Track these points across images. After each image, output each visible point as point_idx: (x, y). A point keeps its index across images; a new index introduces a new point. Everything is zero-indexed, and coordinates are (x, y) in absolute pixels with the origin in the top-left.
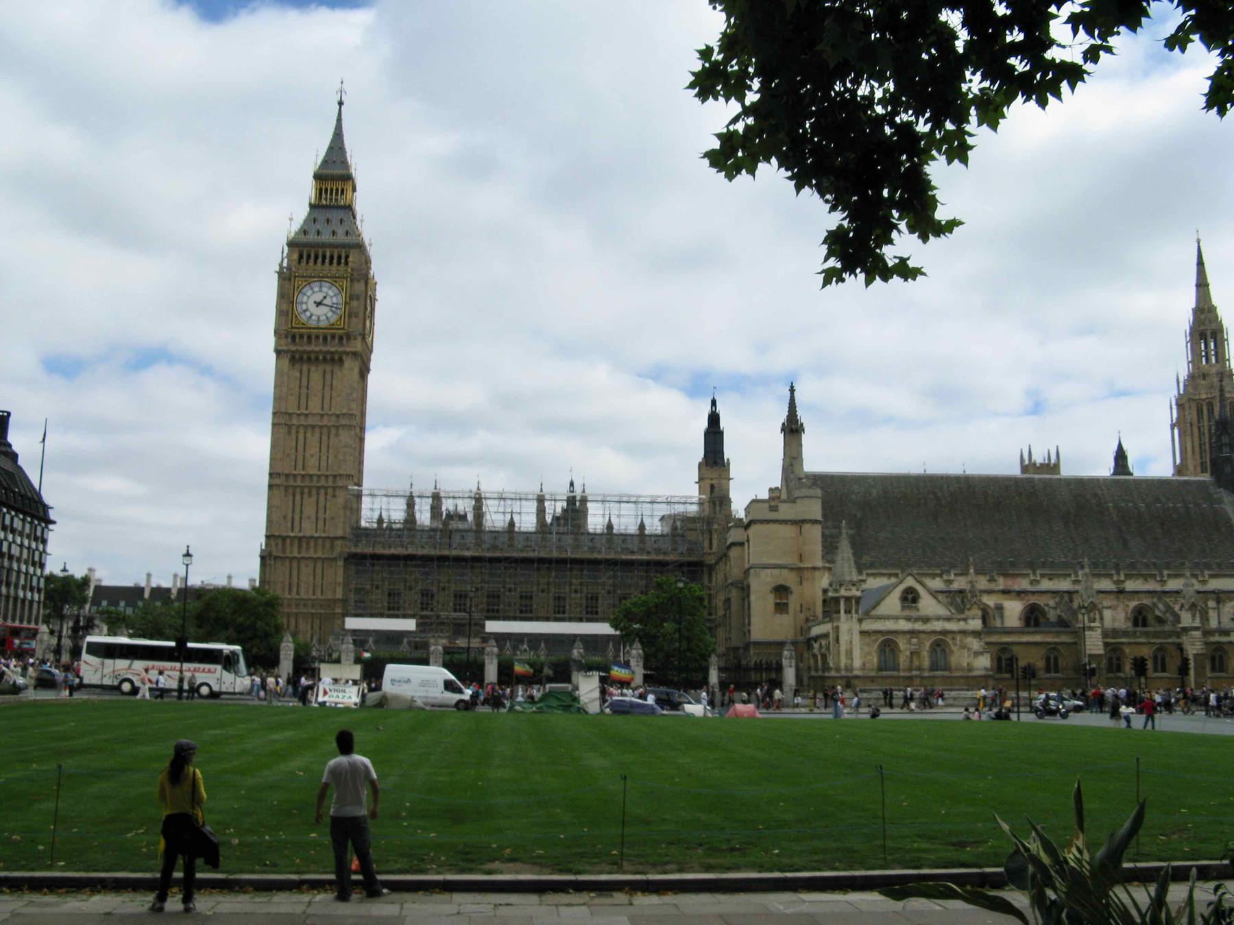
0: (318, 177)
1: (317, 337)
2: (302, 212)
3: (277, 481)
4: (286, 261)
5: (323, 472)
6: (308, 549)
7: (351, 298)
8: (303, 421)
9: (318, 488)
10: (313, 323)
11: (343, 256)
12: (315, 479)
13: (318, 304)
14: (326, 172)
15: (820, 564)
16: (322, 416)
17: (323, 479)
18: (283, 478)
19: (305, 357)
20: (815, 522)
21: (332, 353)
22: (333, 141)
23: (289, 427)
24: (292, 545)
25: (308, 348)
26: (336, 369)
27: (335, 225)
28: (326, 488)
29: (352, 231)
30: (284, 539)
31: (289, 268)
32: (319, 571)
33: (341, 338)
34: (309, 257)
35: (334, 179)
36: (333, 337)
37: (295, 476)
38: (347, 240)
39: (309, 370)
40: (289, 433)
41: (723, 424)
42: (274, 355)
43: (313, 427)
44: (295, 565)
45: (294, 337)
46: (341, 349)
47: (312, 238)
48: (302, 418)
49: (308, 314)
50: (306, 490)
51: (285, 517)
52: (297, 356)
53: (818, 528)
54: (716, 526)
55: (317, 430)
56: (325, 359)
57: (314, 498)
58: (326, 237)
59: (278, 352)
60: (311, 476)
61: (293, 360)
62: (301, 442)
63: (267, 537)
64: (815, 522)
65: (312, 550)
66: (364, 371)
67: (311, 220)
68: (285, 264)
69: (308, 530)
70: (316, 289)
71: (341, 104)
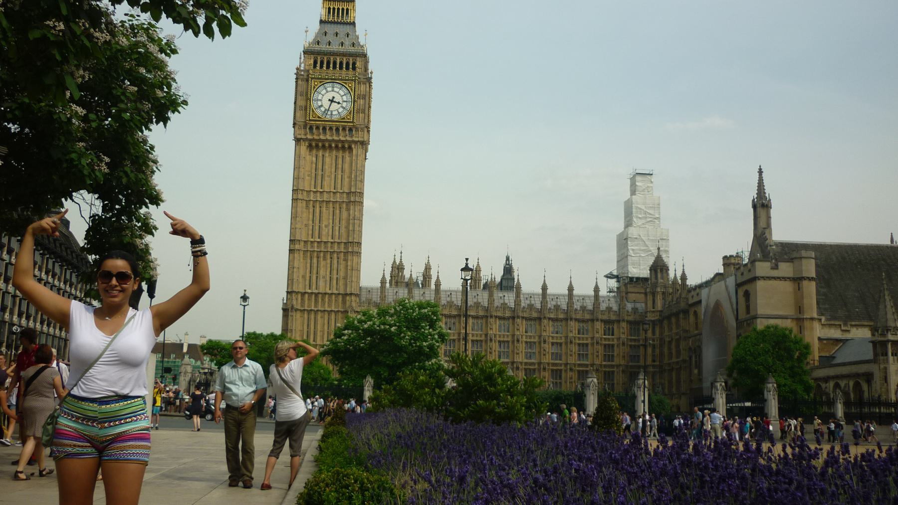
2: (315, 27)
3: (297, 247)
4: (303, 65)
10: (328, 118)
12: (329, 245)
13: (332, 101)
15: (815, 315)
18: (302, 244)
19: (320, 144)
20: (810, 279)
21: (343, 142)
23: (308, 202)
24: (309, 300)
25: (322, 137)
28: (338, 253)
30: (303, 294)
34: (322, 63)
37: (312, 242)
38: (352, 50)
40: (307, 207)
44: (312, 316)
45: (311, 128)
47: (324, 47)
48: (318, 194)
50: (322, 254)
51: (304, 277)
53: (813, 284)
54: (659, 289)
56: (337, 147)
57: (329, 261)
58: (335, 48)
59: (298, 140)
60: (325, 242)
61: (310, 147)
62: (317, 214)
63: (288, 292)
64: (810, 279)
69: (323, 287)
70: (329, 89)
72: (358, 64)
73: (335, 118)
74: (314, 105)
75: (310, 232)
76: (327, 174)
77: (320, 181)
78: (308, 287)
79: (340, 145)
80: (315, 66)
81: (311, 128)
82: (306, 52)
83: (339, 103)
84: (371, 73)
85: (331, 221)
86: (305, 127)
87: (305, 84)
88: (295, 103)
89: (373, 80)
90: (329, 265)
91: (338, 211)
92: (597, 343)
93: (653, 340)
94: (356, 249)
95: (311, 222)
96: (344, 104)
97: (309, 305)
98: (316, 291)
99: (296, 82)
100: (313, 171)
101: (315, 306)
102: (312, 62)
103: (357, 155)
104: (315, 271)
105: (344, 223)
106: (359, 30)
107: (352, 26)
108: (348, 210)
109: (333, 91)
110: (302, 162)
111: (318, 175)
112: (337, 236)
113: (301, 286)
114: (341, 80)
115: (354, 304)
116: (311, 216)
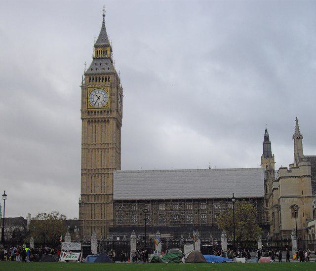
0: (96, 46)
1: (98, 112)
3: (83, 173)
4: (84, 81)
6: (98, 200)
7: (111, 95)
8: (94, 147)
10: (96, 106)
11: (107, 78)
12: (100, 170)
14: (98, 44)
16: (102, 144)
17: (103, 171)
19: (94, 120)
22: (102, 31)
24: (91, 198)
26: (106, 125)
27: (104, 66)
30: (88, 196)
31: (85, 84)
32: (103, 209)
33: (108, 112)
34: (93, 79)
35: (103, 49)
37: (92, 169)
41: (270, 140)
42: (81, 120)
43: (98, 149)
44: (93, 207)
47: (94, 71)
52: (90, 120)
54: (268, 183)
55: (100, 150)
56: (102, 121)
57: (100, 179)
59: (83, 119)
60: (98, 169)
61: (89, 121)
63: (82, 195)
65: (100, 200)
66: (119, 125)
67: (94, 64)
68: (84, 83)
71: (104, 16)
73: (100, 107)
74: (91, 100)
86: (86, 112)
97: (92, 201)
98: (95, 194)
101: (95, 201)
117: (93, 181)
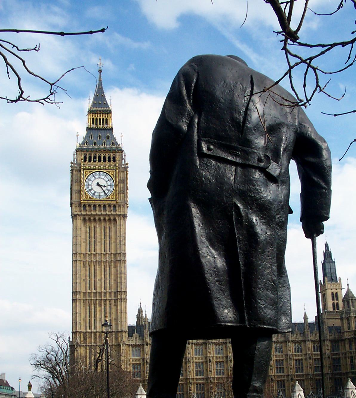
2: (83, 133)
5: (108, 290)
7: (119, 182)
9: (105, 301)
10: (96, 197)
11: (112, 157)
18: (82, 294)
19: (92, 218)
21: (109, 215)
25: (93, 213)
28: (110, 300)
29: (114, 143)
30: (85, 333)
36: (110, 206)
39: (95, 227)
40: (85, 266)
43: (100, 262)
45: (85, 206)
46: (114, 213)
47: (91, 146)
48: (92, 256)
49: (92, 192)
50: (97, 302)
56: (104, 219)
57: (103, 307)
61: (84, 220)
63: (73, 333)
70: (97, 177)
72: (117, 158)
73: (101, 198)
74: (86, 189)
75: (88, 285)
76: (98, 240)
77: (93, 246)
78: (88, 328)
79: (107, 218)
80: (85, 160)
81: (85, 206)
82: (78, 150)
83: (104, 186)
84: (127, 164)
85: (103, 276)
87: (77, 174)
88: (71, 188)
89: (128, 169)
90: (103, 310)
91: (108, 269)
92: (310, 358)
93: (351, 353)
94: (123, 296)
95: (88, 278)
96: (109, 188)
98: (95, 331)
99: (72, 173)
100: (88, 238)
102: (83, 157)
103: (120, 225)
104: (93, 315)
105: (113, 277)
106: (116, 133)
107: (110, 131)
108: (116, 267)
109: (100, 178)
110: (79, 232)
111: (91, 241)
112: (108, 288)
113: (82, 327)
114: (106, 169)
115: (124, 339)
116: (88, 273)
117: (93, 311)
